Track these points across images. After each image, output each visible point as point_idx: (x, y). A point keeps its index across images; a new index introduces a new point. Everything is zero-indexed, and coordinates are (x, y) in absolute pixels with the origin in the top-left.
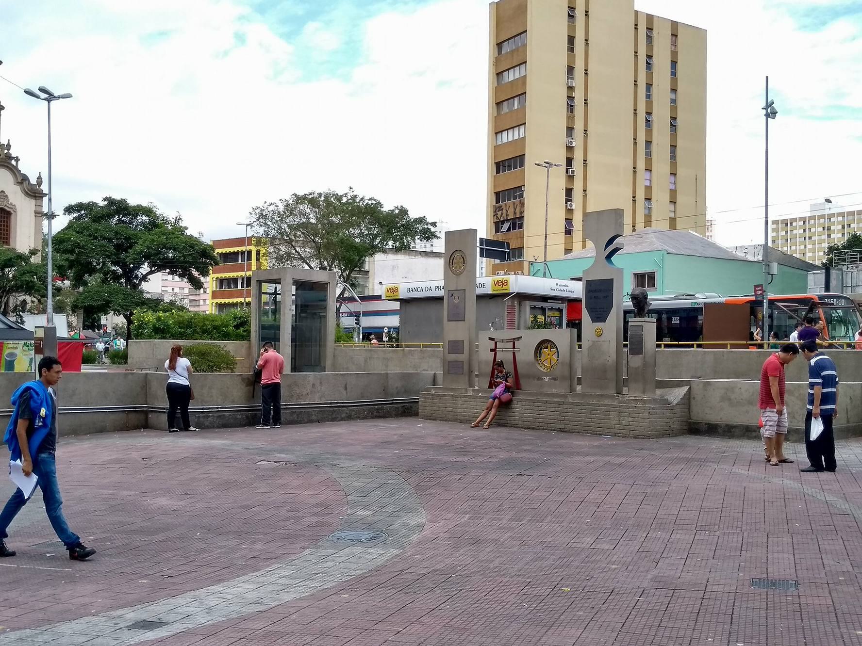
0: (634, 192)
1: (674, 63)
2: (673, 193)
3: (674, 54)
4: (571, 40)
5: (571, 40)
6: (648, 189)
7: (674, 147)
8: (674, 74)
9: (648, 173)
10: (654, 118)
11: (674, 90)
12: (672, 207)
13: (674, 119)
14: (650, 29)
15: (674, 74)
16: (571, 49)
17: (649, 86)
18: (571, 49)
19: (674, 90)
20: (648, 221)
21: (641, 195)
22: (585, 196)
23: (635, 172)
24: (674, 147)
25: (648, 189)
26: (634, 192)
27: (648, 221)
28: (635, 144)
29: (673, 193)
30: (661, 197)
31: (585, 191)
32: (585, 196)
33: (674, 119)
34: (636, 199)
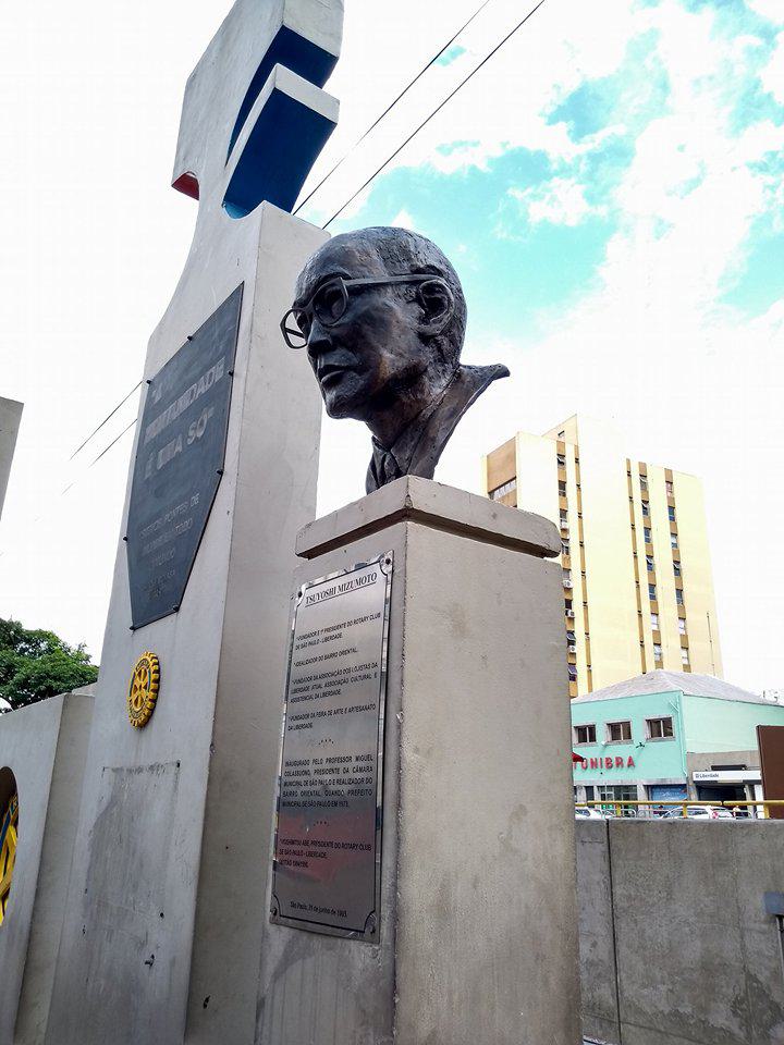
0: (642, 636)
1: (672, 509)
2: (684, 638)
3: (671, 500)
4: (562, 485)
5: (562, 485)
6: (657, 633)
7: (679, 592)
8: (672, 519)
9: (655, 617)
10: (656, 561)
11: (674, 535)
12: (684, 653)
13: (677, 562)
14: (643, 476)
15: (672, 519)
16: (563, 493)
17: (647, 530)
18: (563, 493)
19: (674, 535)
20: (659, 664)
21: (649, 640)
22: (588, 639)
23: (640, 616)
24: (679, 592)
25: (657, 633)
26: (642, 636)
27: (659, 664)
28: (638, 586)
29: (684, 638)
30: (671, 642)
31: (587, 634)
32: (588, 639)
33: (677, 562)
34: (645, 643)
